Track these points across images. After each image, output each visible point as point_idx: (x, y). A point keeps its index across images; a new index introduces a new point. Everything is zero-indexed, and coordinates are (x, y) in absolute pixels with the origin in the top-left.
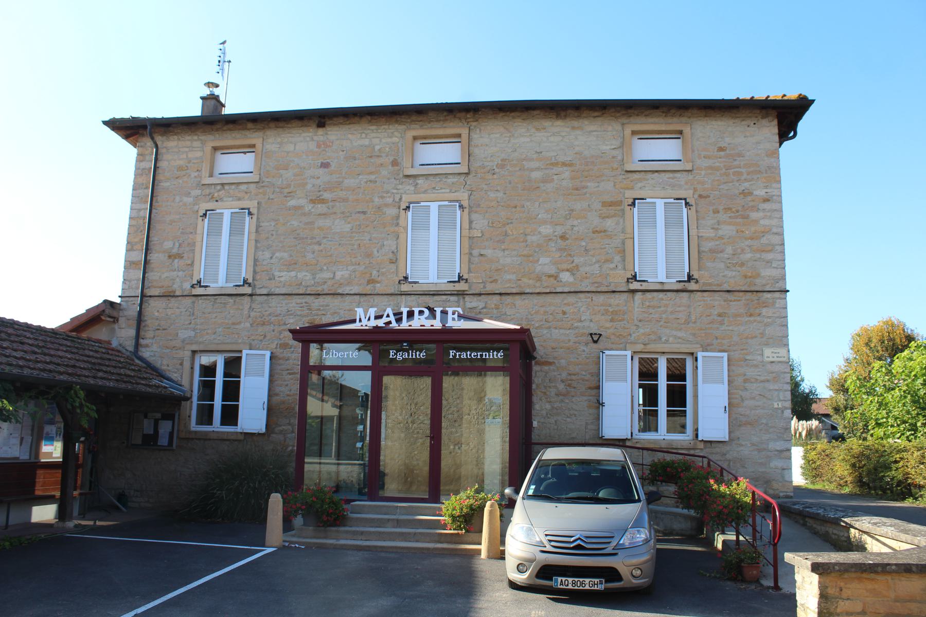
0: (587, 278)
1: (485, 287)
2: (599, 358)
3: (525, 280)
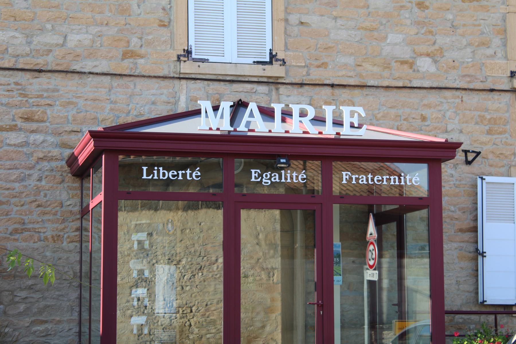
0: (454, 68)
1: (308, 74)
2: (476, 186)
3: (367, 66)
